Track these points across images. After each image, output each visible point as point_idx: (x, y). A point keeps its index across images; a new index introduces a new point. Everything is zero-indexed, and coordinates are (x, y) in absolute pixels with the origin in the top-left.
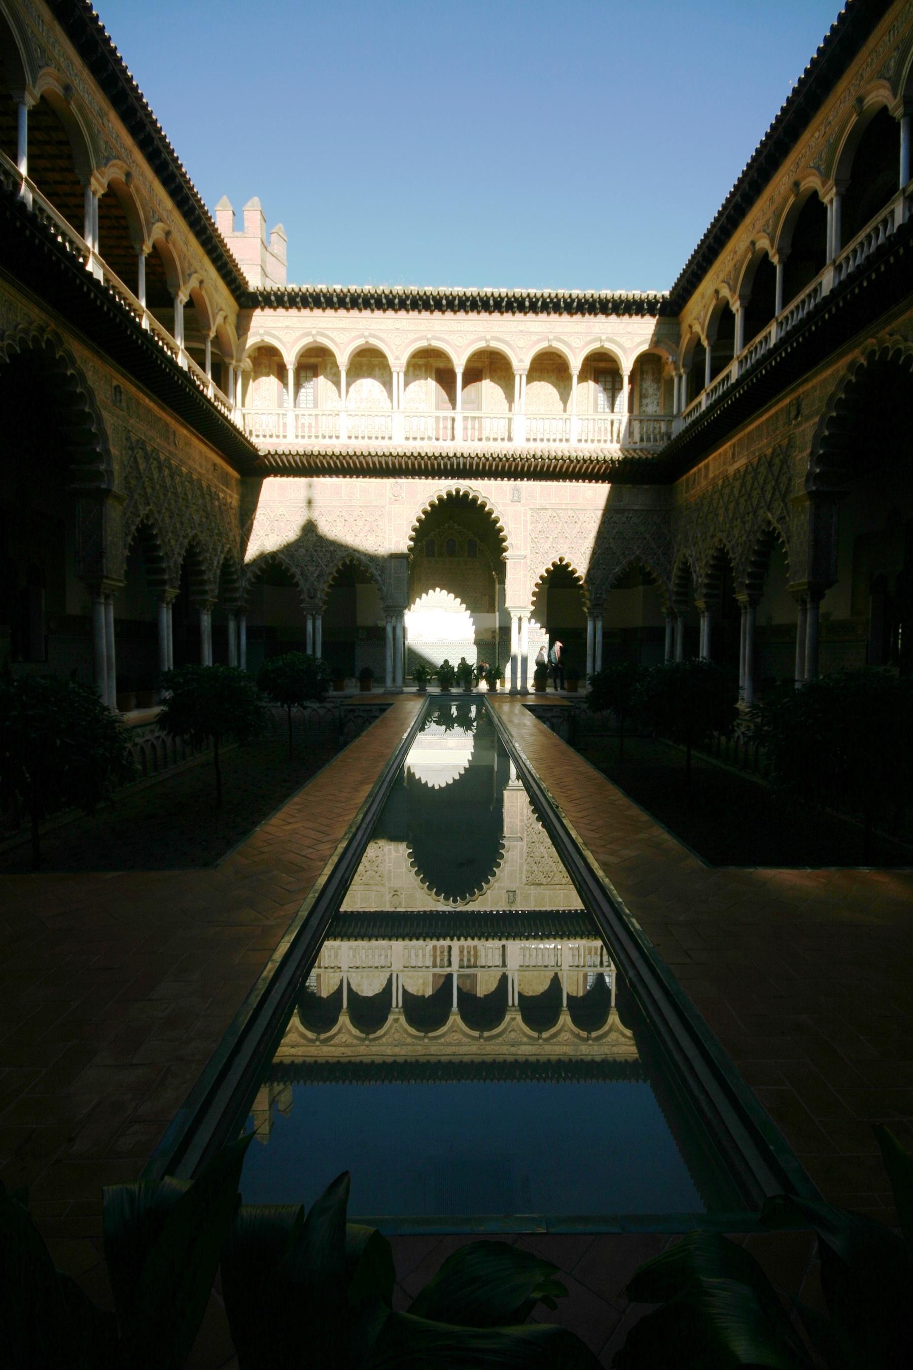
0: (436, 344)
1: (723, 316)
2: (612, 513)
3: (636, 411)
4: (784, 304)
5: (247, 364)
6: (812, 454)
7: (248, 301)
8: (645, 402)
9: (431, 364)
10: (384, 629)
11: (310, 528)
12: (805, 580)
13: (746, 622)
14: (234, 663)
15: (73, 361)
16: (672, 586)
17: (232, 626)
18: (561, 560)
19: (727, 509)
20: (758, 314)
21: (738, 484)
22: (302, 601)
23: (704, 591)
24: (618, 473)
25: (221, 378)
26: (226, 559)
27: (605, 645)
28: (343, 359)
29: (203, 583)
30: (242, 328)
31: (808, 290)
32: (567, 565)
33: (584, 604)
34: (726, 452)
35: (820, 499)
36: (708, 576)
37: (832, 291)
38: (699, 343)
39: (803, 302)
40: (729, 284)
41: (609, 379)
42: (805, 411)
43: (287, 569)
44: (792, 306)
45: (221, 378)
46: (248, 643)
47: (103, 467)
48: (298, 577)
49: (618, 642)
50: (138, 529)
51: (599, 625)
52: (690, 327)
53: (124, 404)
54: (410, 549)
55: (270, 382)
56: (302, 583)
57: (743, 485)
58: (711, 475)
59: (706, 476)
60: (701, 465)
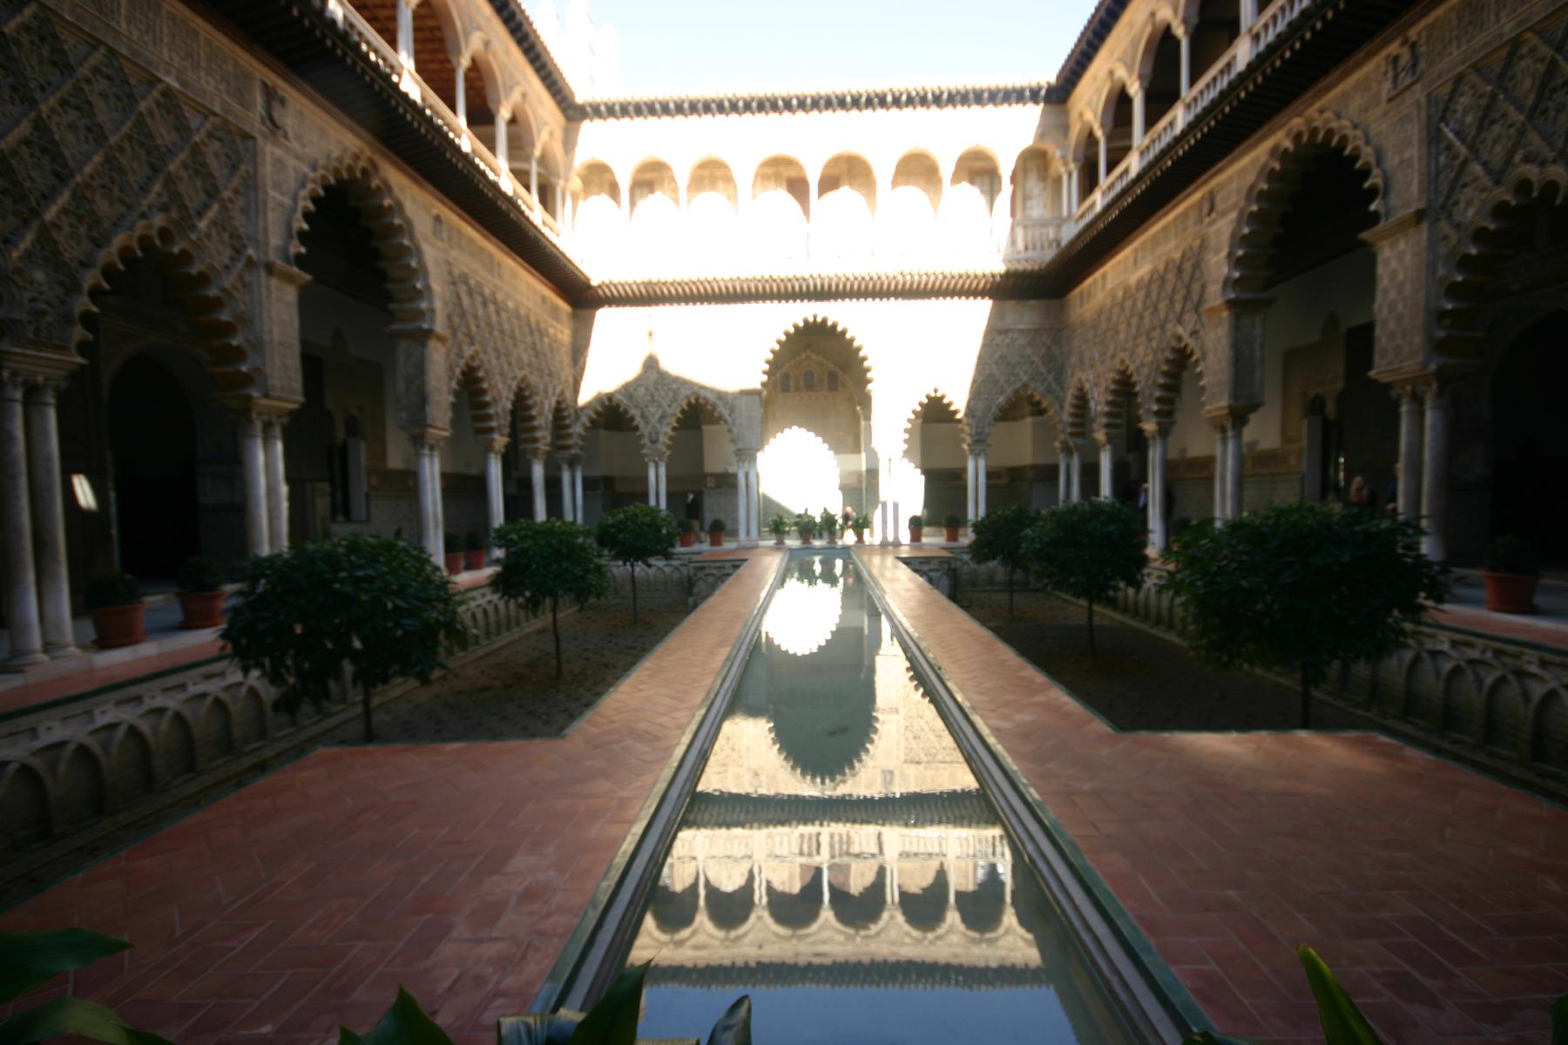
1: (1120, 103)
2: (994, 332)
3: (1019, 216)
4: (1193, 80)
5: (576, 183)
6: (1230, 255)
7: (573, 113)
8: (1029, 204)
10: (735, 476)
11: (651, 364)
12: (1224, 403)
13: (1155, 455)
14: (569, 517)
15: (389, 189)
16: (1066, 417)
19: (1129, 325)
20: (1161, 97)
21: (1141, 295)
22: (643, 446)
23: (1104, 420)
25: (547, 197)
26: (558, 403)
27: (989, 487)
28: (682, 174)
29: (534, 429)
30: (569, 144)
31: (1220, 64)
32: (943, 397)
33: (963, 440)
34: (1126, 259)
35: (1237, 307)
36: (1109, 403)
37: (1249, 65)
38: (1091, 135)
39: (1215, 79)
40: (1125, 63)
41: (987, 180)
42: (1220, 206)
43: (626, 411)
44: (1201, 84)
45: (547, 197)
46: (585, 496)
48: (638, 421)
49: (1003, 482)
50: (463, 373)
52: (1081, 115)
53: (445, 235)
54: (763, 385)
56: (642, 426)
57: (1148, 295)
58: (1109, 286)
59: (1104, 287)
60: (1098, 274)
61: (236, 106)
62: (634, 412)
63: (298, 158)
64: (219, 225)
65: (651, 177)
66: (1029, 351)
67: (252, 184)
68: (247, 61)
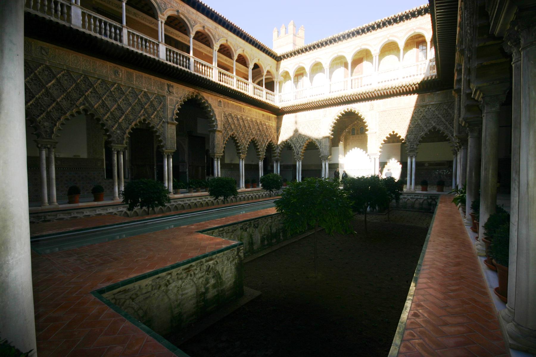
0: (340, 54)
2: (418, 107)
5: (282, 78)
7: (278, 59)
9: (339, 61)
11: (296, 131)
17: (275, 165)
18: (393, 132)
24: (424, 88)
30: (277, 68)
32: (397, 134)
47: (214, 124)
48: (294, 148)
51: (414, 160)
53: (222, 105)
54: (332, 135)
55: (342, 69)
61: (160, 91)
62: (292, 145)
63: (176, 97)
64: (156, 116)
65: (300, 73)
66: (437, 113)
67: (165, 106)
68: (163, 81)
